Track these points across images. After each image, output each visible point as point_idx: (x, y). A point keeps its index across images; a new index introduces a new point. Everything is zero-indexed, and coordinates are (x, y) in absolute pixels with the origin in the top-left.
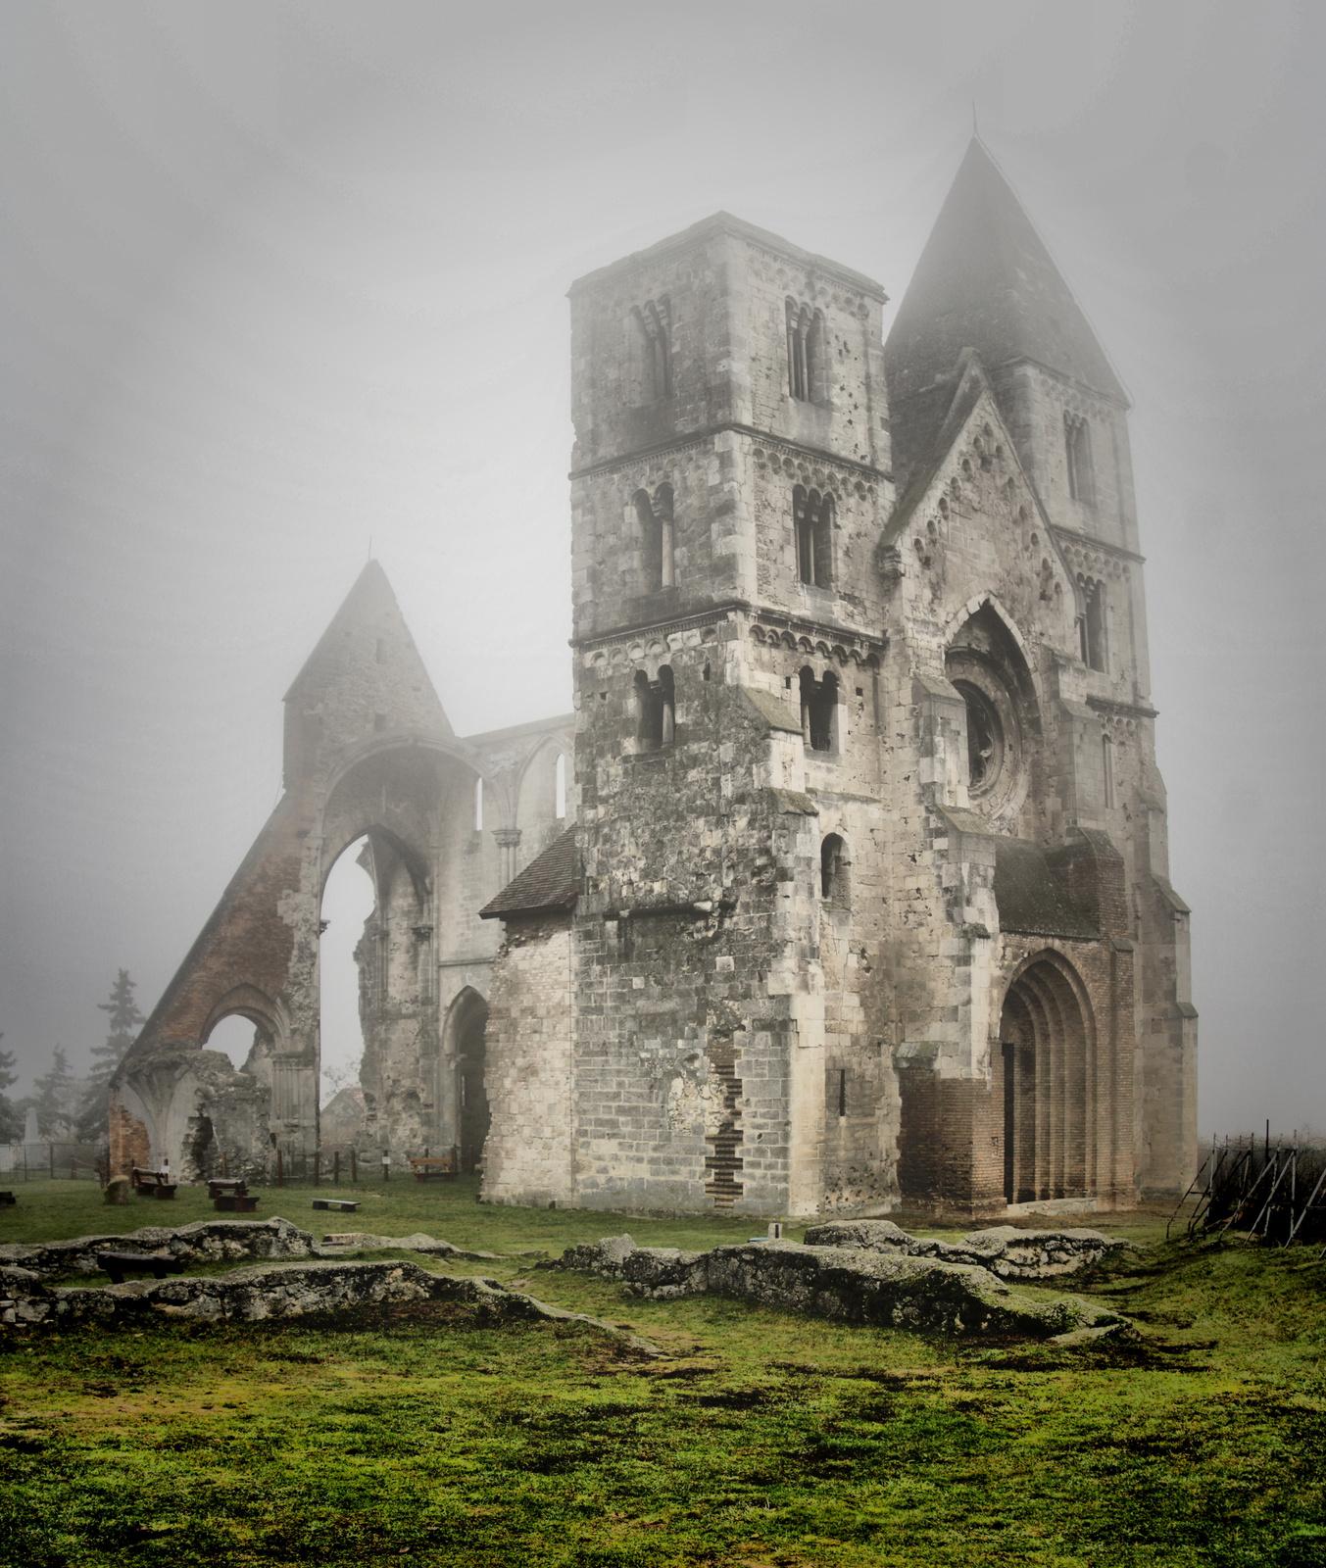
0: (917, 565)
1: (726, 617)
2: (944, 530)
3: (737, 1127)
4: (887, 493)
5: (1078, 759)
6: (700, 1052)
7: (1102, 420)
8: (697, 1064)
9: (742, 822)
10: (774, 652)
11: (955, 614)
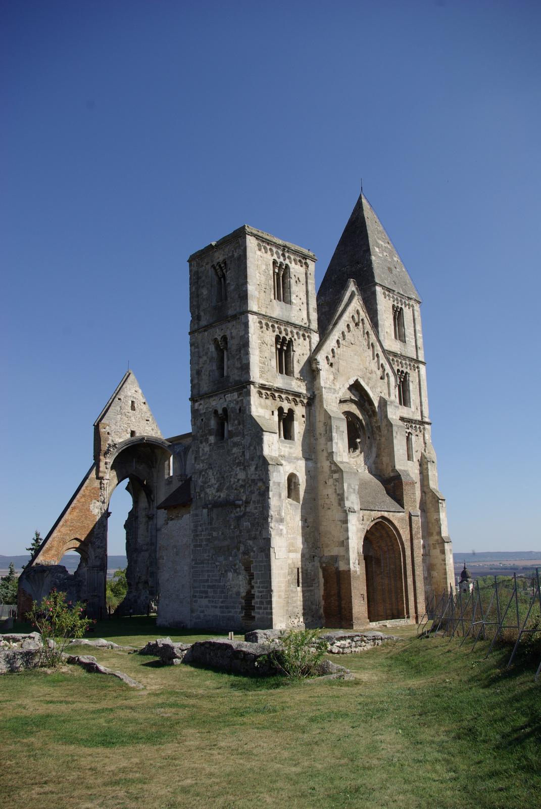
0: (327, 366)
1: (247, 388)
2: (339, 352)
3: (252, 593)
4: (315, 338)
5: (395, 441)
6: (238, 561)
7: (409, 308)
8: (237, 567)
9: (253, 468)
10: (267, 401)
11: (343, 385)
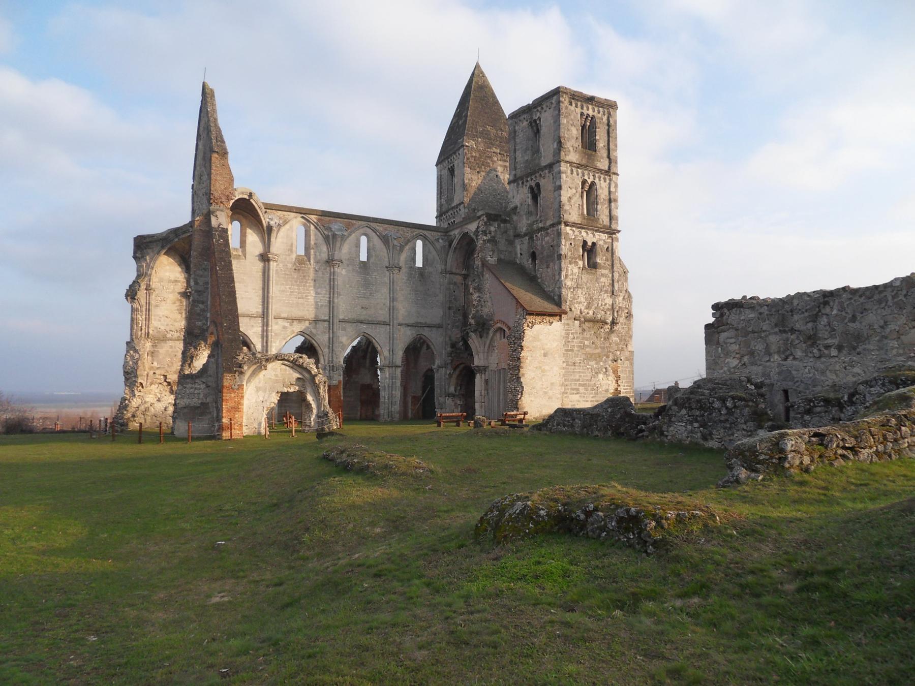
9: (621, 298)
